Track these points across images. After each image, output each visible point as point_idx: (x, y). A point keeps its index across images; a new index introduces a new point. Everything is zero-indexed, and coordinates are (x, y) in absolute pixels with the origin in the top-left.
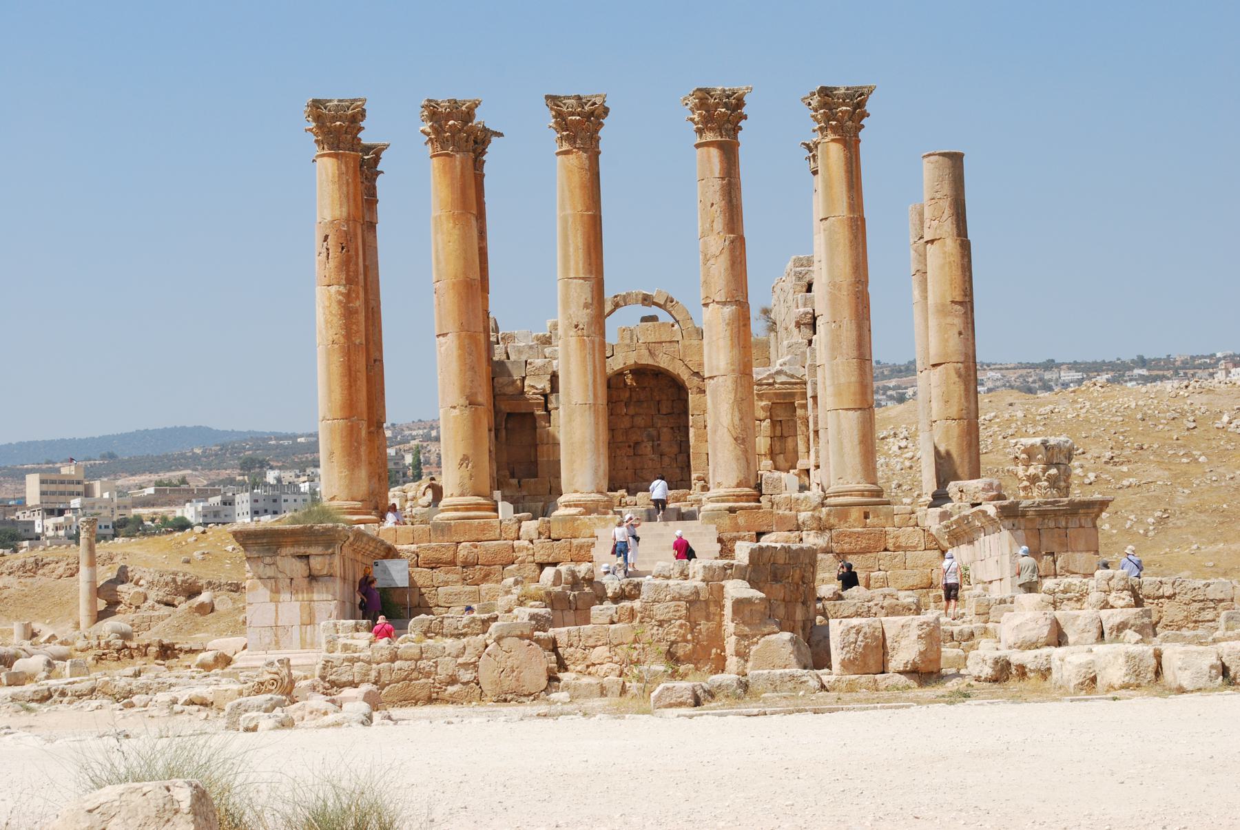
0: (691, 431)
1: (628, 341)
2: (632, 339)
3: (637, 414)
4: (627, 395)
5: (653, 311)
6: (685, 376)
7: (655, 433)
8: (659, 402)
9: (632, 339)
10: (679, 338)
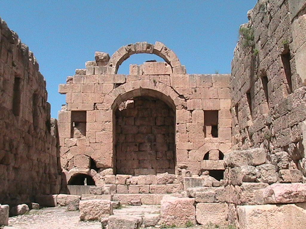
0: (177, 135)
1: (136, 74)
2: (138, 72)
3: (142, 125)
4: (136, 113)
5: (154, 57)
6: (174, 97)
7: (152, 137)
8: (156, 118)
9: (138, 72)
10: (170, 72)
